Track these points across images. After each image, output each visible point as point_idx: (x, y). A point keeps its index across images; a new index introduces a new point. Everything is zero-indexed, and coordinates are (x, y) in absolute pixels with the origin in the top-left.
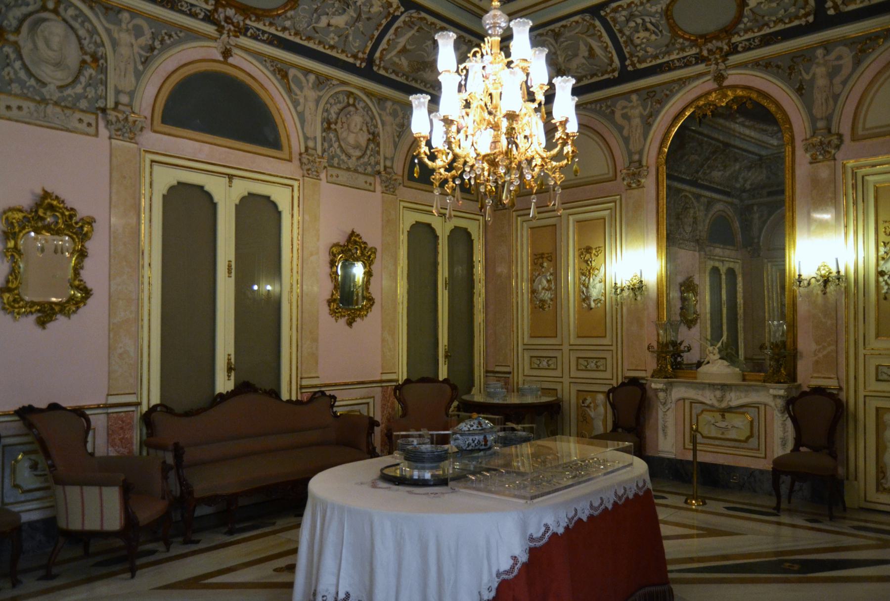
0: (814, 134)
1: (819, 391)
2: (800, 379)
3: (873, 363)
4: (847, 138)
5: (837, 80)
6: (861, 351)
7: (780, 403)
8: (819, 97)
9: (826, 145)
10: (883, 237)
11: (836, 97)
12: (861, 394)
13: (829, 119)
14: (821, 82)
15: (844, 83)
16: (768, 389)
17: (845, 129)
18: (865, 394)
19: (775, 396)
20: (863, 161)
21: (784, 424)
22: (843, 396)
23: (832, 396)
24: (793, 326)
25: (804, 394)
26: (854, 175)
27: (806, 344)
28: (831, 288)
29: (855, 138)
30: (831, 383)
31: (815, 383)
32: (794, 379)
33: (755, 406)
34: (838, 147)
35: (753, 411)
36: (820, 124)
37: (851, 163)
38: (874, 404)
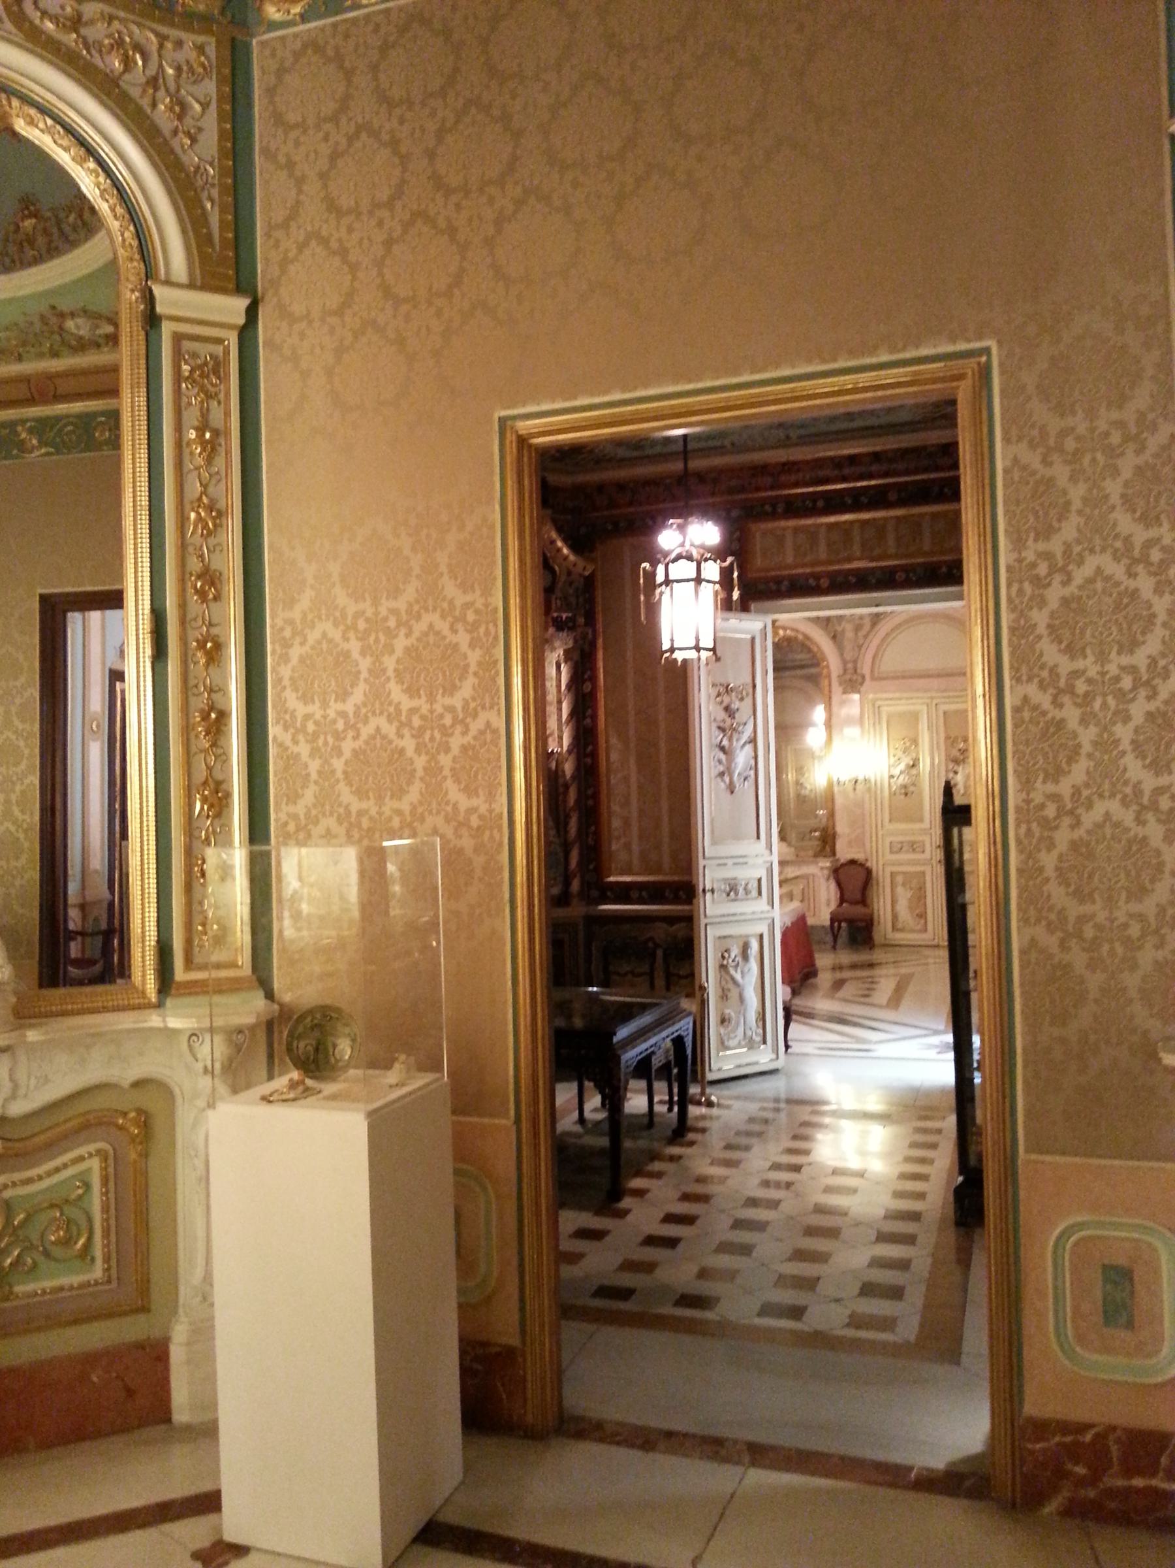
0: (845, 670)
1: (853, 862)
2: (838, 855)
3: (888, 840)
4: (868, 677)
5: (861, 634)
6: (880, 833)
7: (826, 872)
8: (848, 646)
9: (853, 682)
10: (892, 751)
11: (860, 647)
12: (881, 863)
13: (855, 662)
14: (849, 634)
15: (866, 637)
16: (817, 863)
17: (866, 670)
18: (884, 863)
19: (822, 868)
20: (879, 695)
21: (828, 887)
22: (869, 864)
23: (862, 865)
24: (832, 815)
25: (843, 865)
26: (874, 705)
27: (842, 827)
28: (859, 787)
29: (873, 678)
30: (859, 856)
31: (849, 857)
32: (834, 853)
33: (805, 877)
34: (861, 684)
35: (805, 881)
36: (850, 666)
37: (871, 696)
38: (888, 870)
